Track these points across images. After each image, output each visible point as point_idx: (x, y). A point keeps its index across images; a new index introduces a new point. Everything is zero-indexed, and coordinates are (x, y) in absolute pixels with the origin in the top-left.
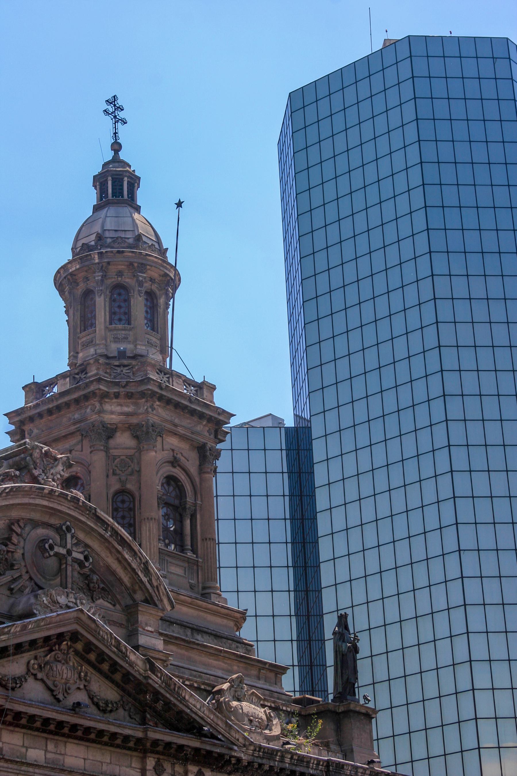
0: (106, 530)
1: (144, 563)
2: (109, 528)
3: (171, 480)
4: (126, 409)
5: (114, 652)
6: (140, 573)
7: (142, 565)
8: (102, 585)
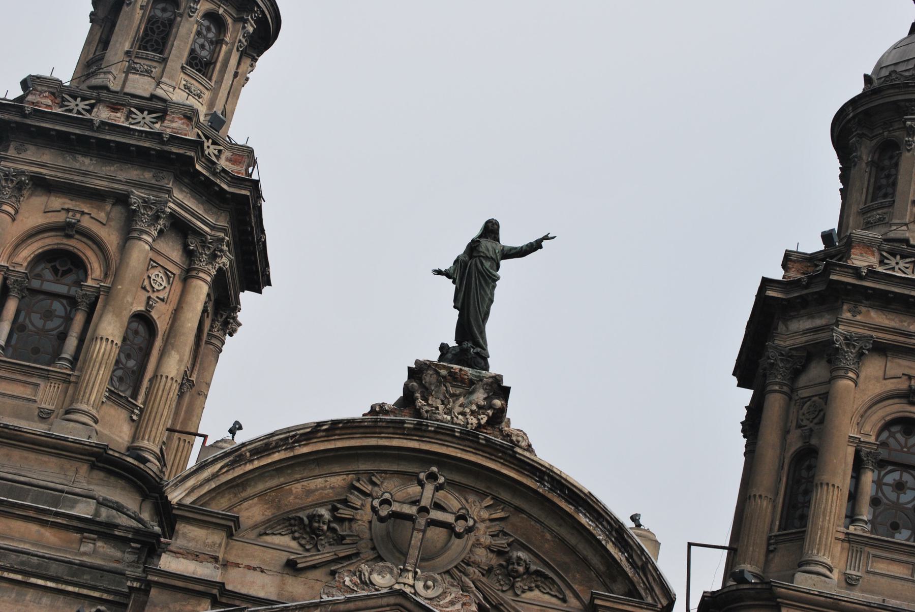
0: (541, 481)
1: (616, 531)
2: (546, 478)
4: (818, 322)
6: (610, 547)
7: (614, 533)
8: (533, 568)
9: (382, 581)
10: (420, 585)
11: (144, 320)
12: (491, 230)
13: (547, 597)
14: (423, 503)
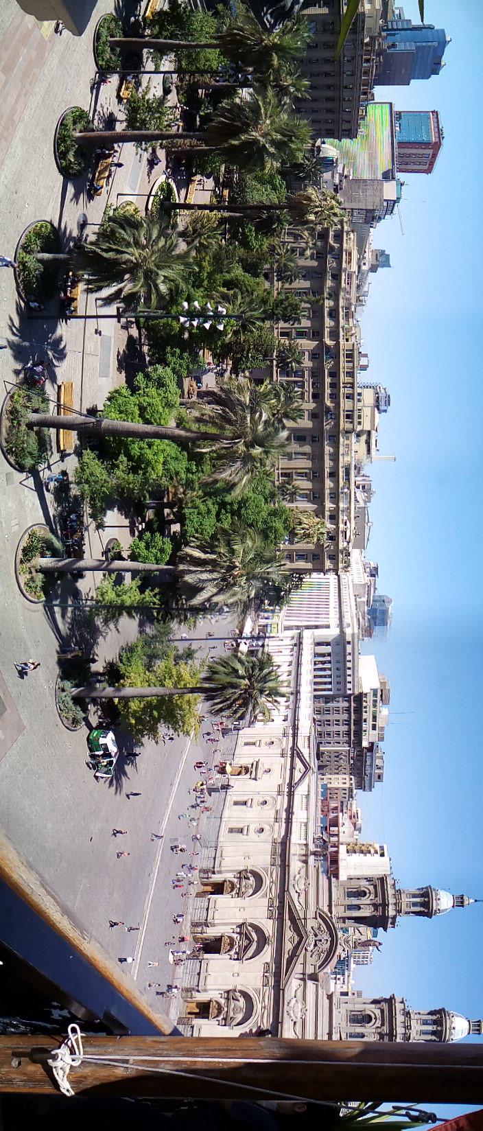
12: (380, 944)
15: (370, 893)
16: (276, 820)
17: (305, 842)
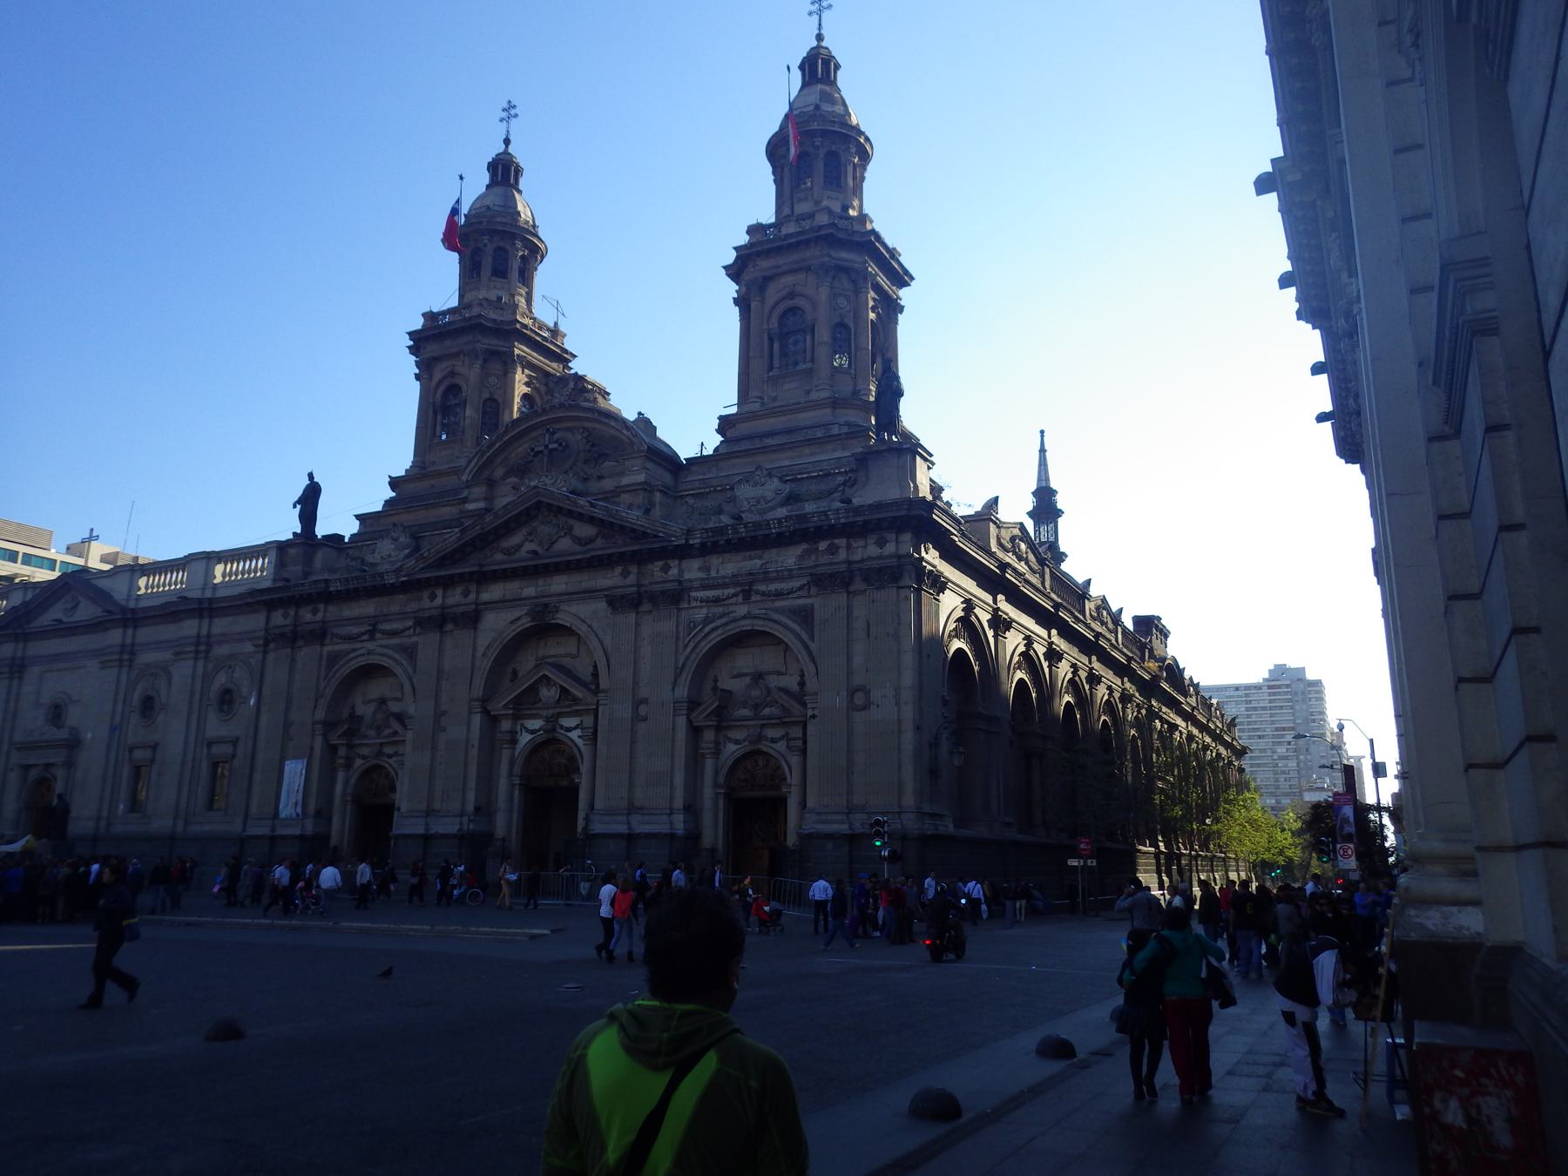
0: (594, 413)
3: (793, 310)
5: (569, 504)
9: (533, 484)
10: (548, 481)
11: (492, 400)
13: (612, 463)
14: (547, 443)
15: (452, 374)
16: (203, 646)
17: (273, 554)
